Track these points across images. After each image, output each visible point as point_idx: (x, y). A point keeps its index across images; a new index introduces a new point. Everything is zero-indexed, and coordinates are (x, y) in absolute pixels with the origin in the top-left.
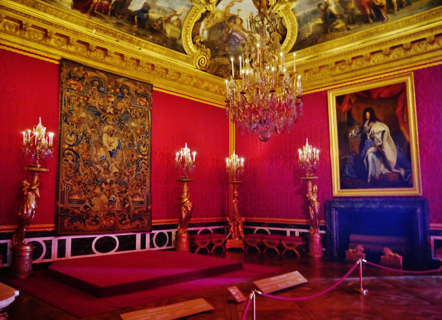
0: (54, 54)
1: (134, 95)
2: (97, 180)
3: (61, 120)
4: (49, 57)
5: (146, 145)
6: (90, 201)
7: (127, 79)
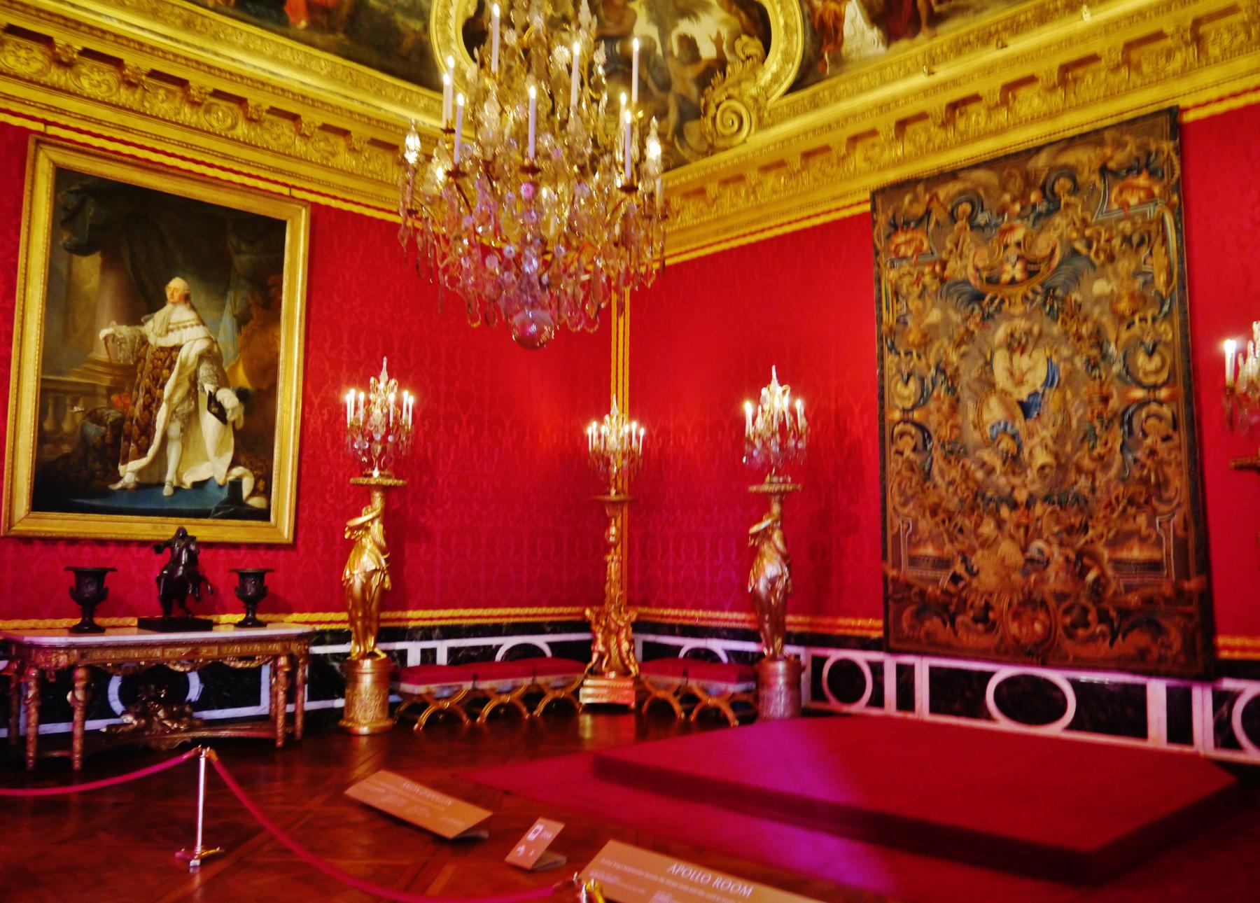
1: (1098, 183)
2: (983, 497)
3: (882, 348)
5: (1160, 348)
6: (965, 561)
7: (1062, 145)
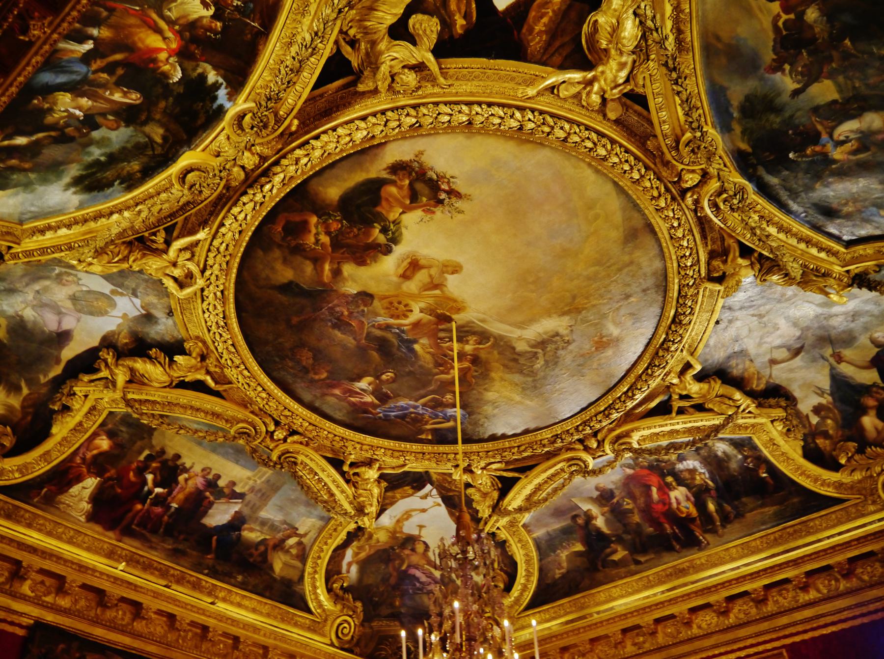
0: (21, 614)
4: (9, 619)
